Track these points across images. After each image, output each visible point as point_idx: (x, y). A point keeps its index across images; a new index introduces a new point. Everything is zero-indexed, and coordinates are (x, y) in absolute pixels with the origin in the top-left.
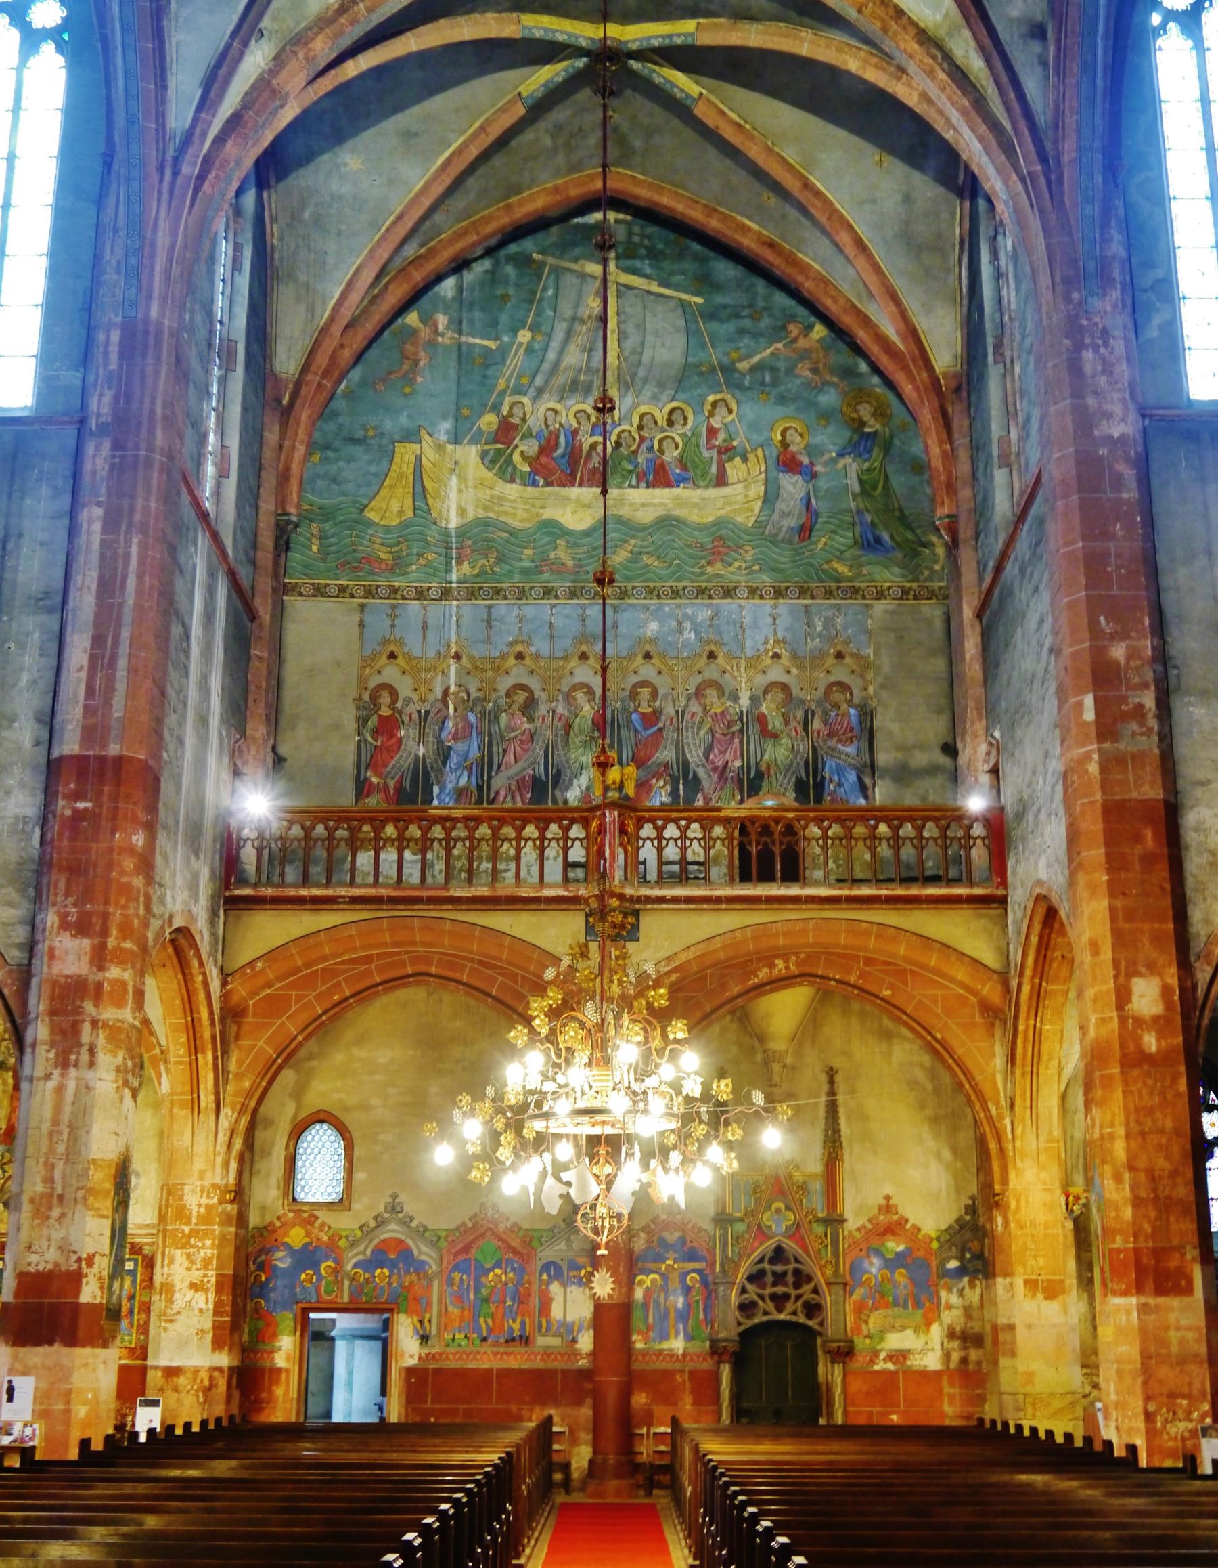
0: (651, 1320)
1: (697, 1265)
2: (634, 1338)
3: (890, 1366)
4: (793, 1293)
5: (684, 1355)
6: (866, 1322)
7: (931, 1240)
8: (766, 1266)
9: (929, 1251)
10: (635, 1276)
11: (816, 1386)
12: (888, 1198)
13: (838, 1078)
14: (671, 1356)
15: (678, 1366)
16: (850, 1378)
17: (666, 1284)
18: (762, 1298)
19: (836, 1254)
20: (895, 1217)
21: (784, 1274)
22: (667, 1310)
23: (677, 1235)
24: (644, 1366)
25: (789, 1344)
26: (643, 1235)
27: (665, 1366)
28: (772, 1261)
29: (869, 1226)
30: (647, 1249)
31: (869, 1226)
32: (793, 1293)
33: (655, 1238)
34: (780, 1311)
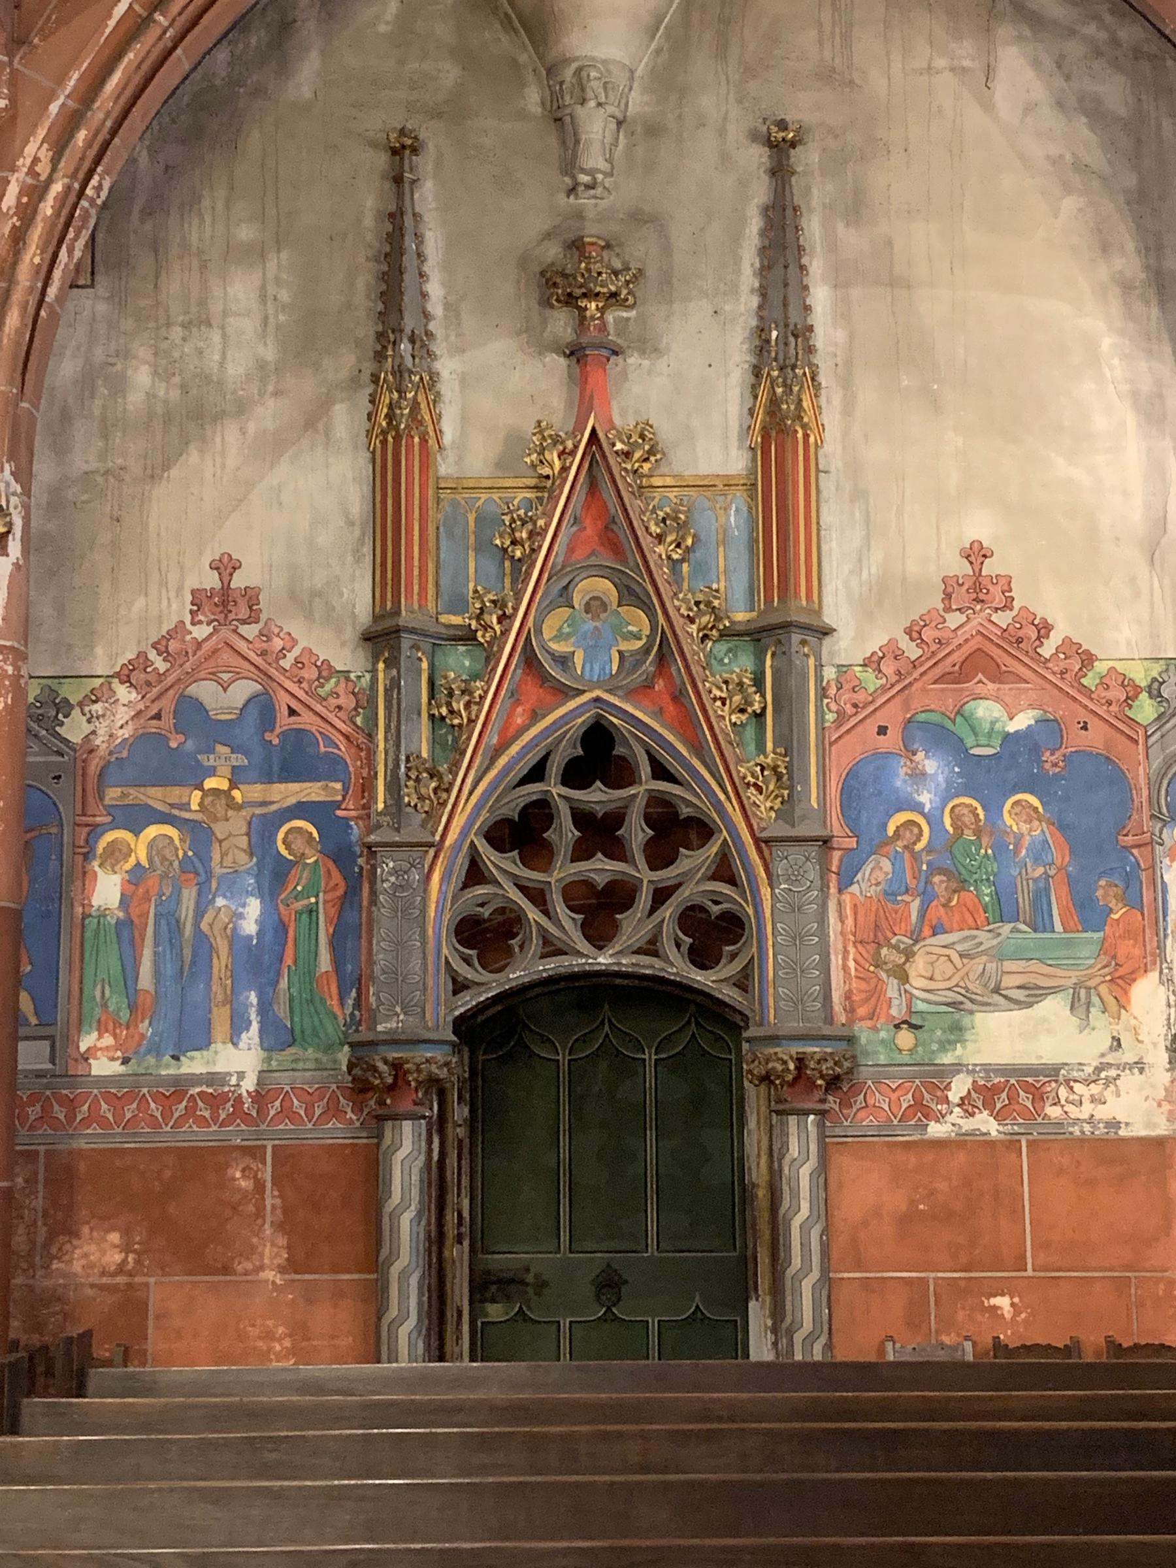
0: (146, 979)
1: (313, 791)
2: (87, 1041)
3: (986, 1124)
4: (647, 878)
5: (259, 1097)
6: (904, 978)
7: (1132, 692)
8: (554, 789)
9: (1128, 730)
10: (95, 831)
11: (746, 1193)
12: (976, 554)
13: (806, 158)
14: (215, 1101)
15: (237, 1133)
16: (845, 1165)
17: (205, 860)
18: (538, 897)
19: (789, 742)
20: (1003, 619)
21: (616, 819)
22: (203, 945)
23: (243, 690)
24: (118, 1140)
25: (649, 1056)
26: (124, 693)
27: (195, 1134)
28: (575, 776)
29: (913, 651)
30: (140, 739)
31: (913, 651)
32: (647, 878)
33: (167, 704)
34: (599, 933)
